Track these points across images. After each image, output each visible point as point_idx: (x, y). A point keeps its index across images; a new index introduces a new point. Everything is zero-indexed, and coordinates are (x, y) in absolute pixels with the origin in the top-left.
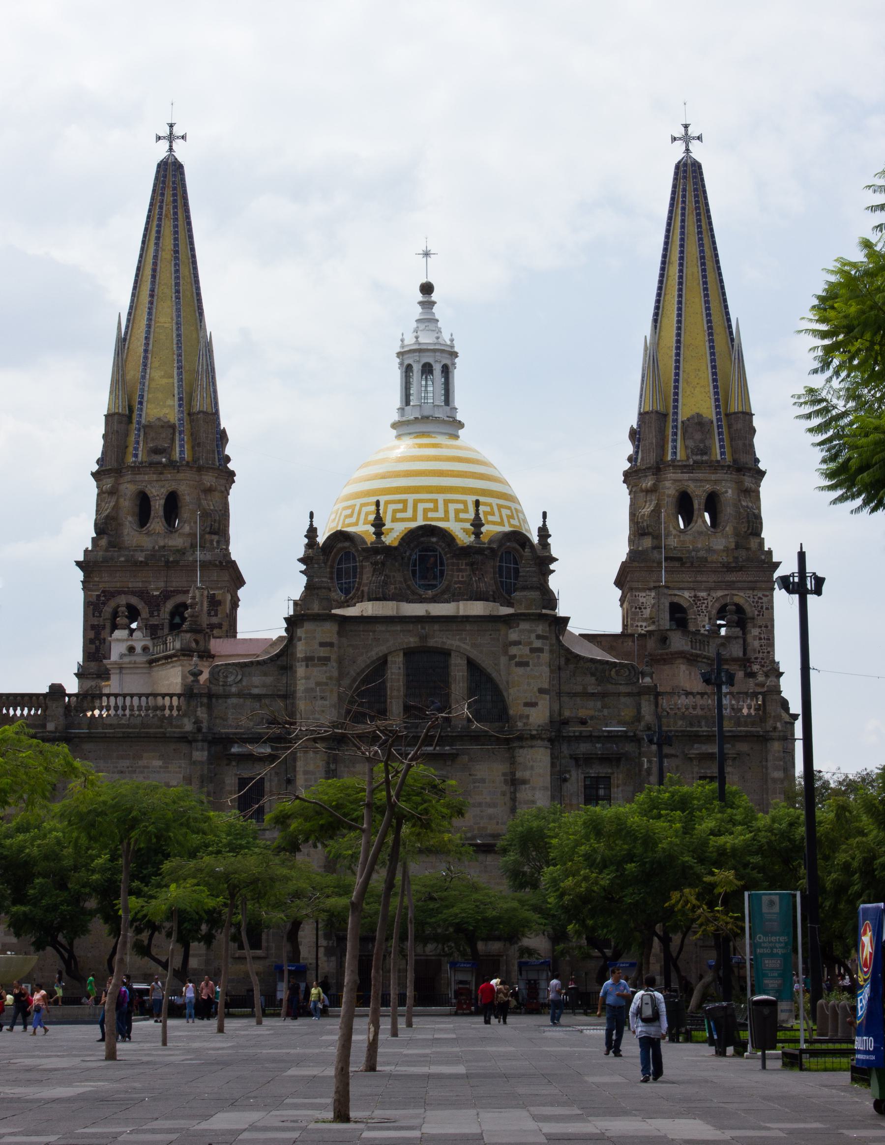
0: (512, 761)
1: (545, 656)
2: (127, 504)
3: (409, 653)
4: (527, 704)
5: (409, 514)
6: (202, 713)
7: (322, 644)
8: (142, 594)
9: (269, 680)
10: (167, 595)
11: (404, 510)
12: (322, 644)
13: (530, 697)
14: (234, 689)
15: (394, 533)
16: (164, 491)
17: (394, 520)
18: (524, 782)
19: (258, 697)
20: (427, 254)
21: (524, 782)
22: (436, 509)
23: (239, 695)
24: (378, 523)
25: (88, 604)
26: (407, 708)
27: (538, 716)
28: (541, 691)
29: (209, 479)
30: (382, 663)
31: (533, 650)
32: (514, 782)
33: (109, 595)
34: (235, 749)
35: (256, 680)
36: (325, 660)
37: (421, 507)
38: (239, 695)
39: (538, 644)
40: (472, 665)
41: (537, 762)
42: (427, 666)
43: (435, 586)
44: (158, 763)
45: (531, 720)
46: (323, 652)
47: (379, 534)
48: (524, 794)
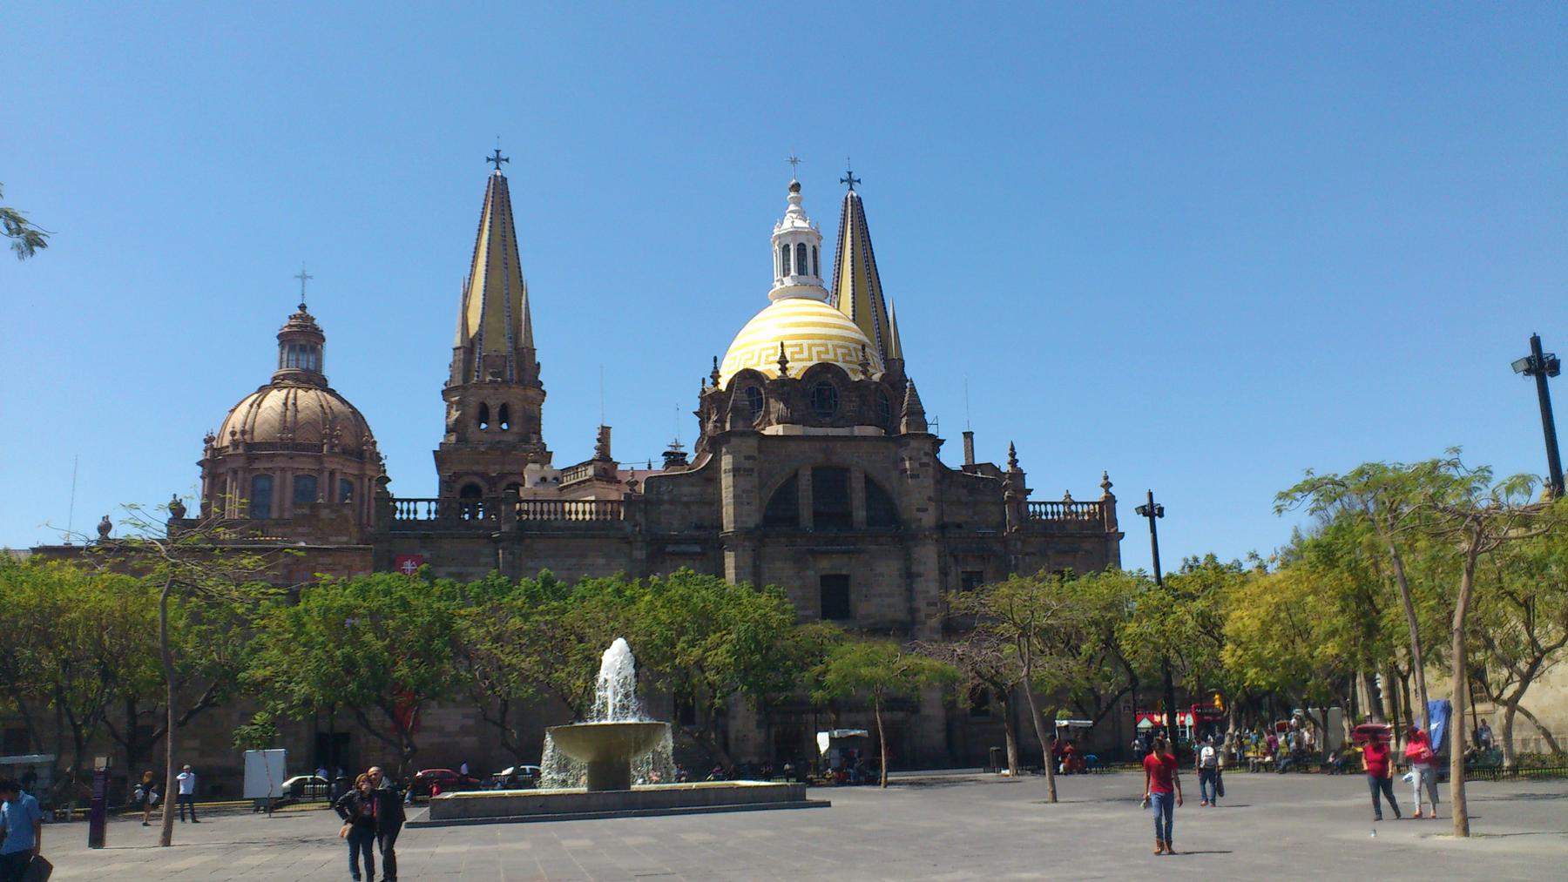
0: (908, 558)
1: (931, 470)
2: (473, 411)
3: (816, 471)
4: (919, 510)
5: (806, 355)
6: (639, 517)
7: (747, 458)
8: (483, 476)
9: (696, 490)
10: (501, 476)
11: (801, 352)
12: (747, 458)
13: (917, 501)
14: (666, 497)
15: (796, 370)
16: (499, 403)
17: (794, 360)
18: (919, 575)
19: (687, 505)
20: (794, 161)
21: (919, 575)
22: (827, 352)
23: (671, 502)
24: (783, 362)
25: (442, 482)
26: (816, 514)
27: (929, 519)
28: (930, 499)
29: (532, 393)
30: (796, 475)
31: (922, 465)
32: (910, 576)
33: (458, 476)
34: (670, 548)
35: (686, 490)
36: (749, 471)
37: (814, 350)
38: (671, 502)
39: (925, 460)
40: (868, 480)
41: (927, 557)
42: (831, 480)
43: (829, 415)
44: (601, 561)
45: (924, 522)
46: (748, 464)
47: (784, 369)
48: (919, 585)
